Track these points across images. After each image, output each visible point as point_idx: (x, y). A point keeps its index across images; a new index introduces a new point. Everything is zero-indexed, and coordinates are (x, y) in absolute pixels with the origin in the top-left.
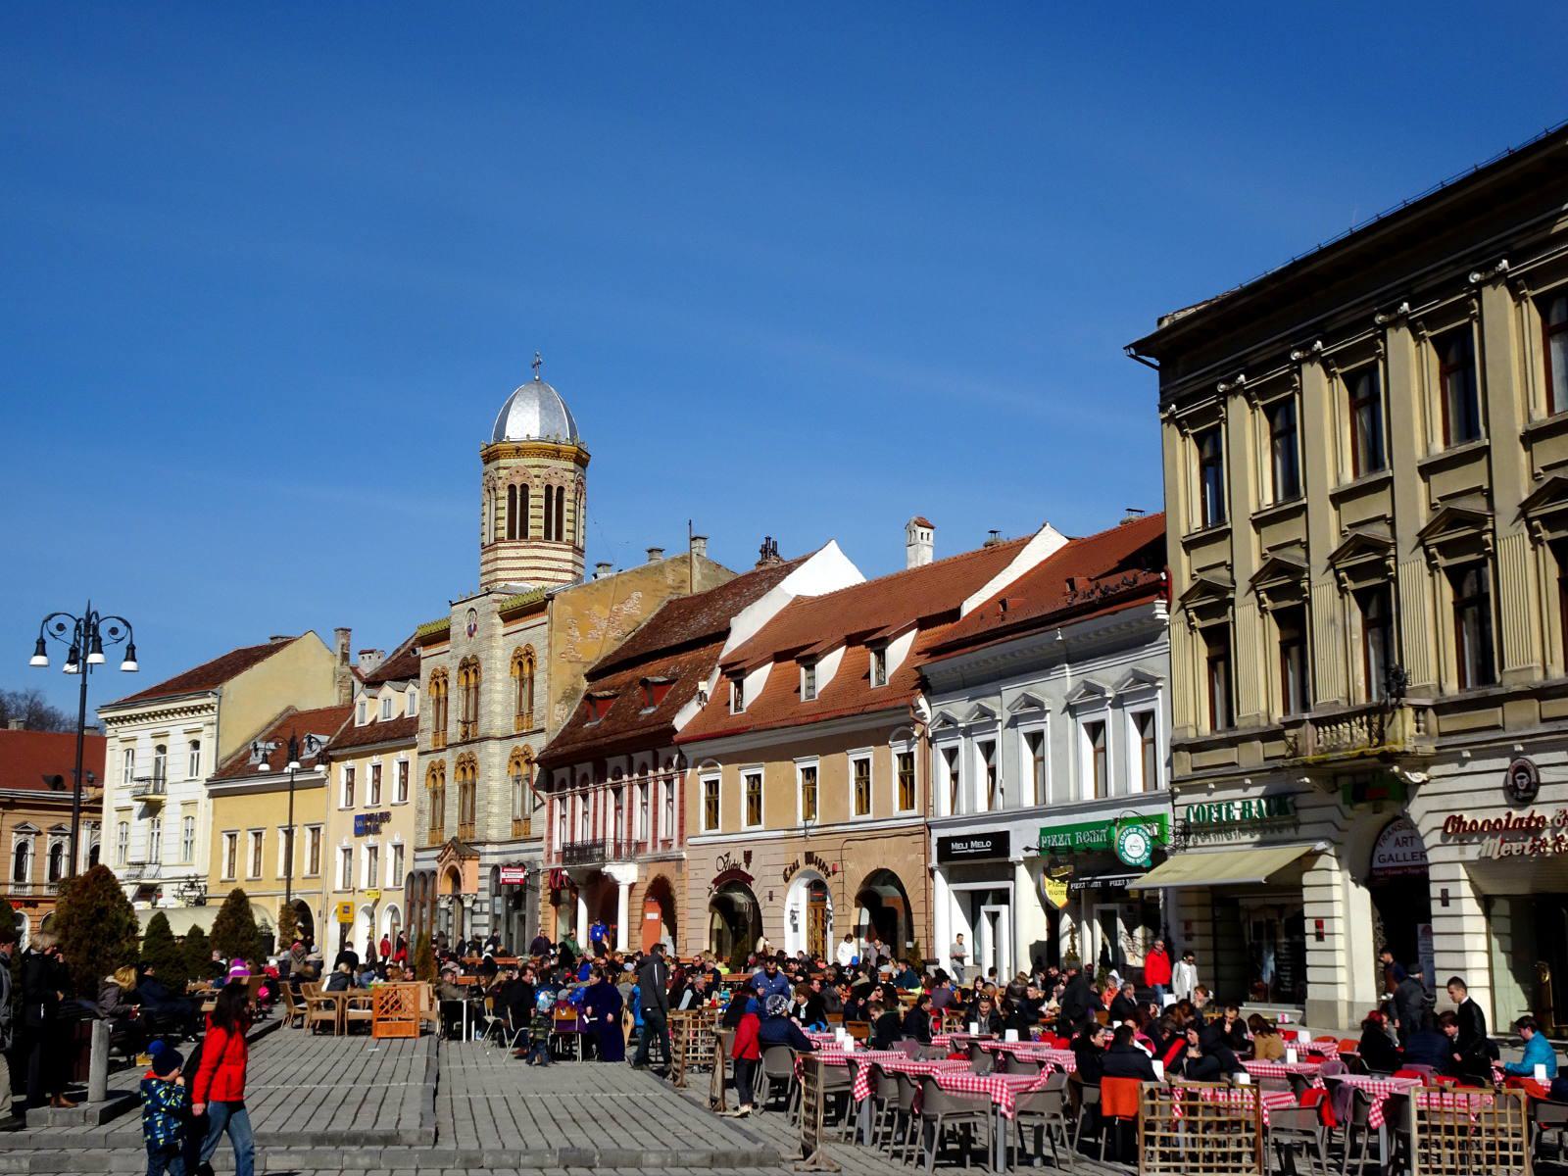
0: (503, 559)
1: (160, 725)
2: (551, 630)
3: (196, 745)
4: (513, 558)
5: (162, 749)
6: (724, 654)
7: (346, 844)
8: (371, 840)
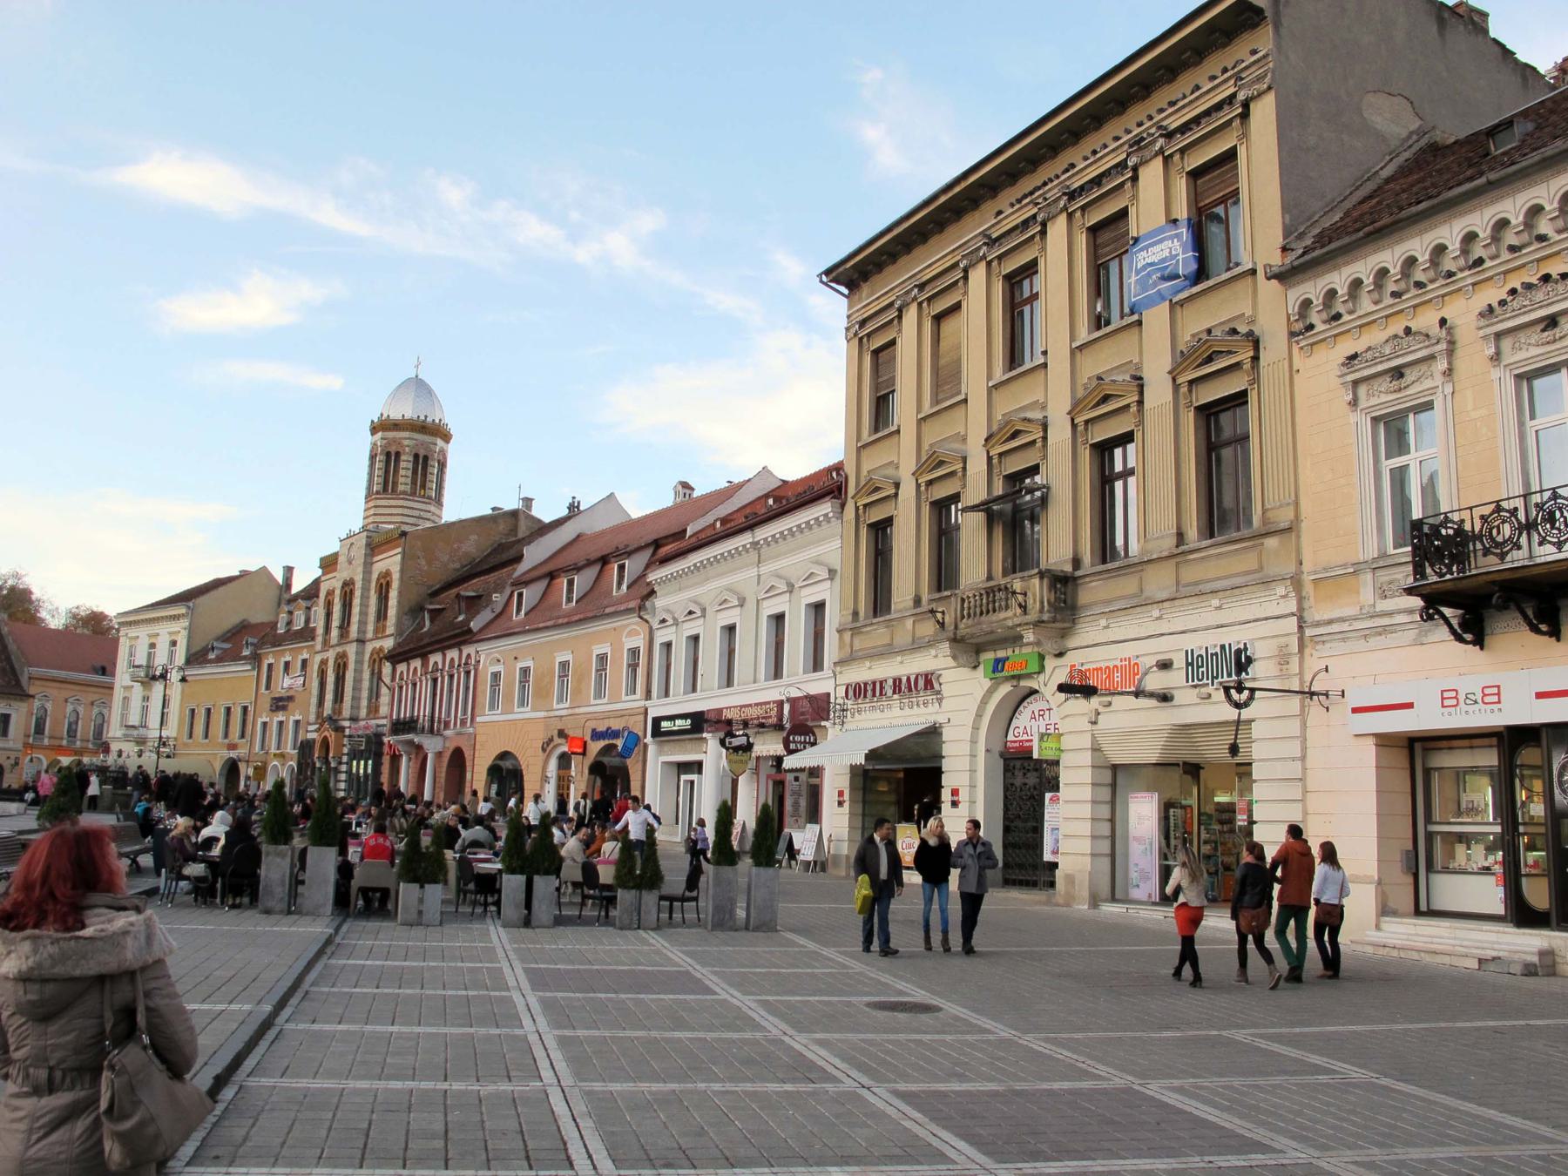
1: (155, 628)
2: (403, 558)
3: (174, 643)
5: (152, 646)
6: (516, 574)
8: (280, 717)
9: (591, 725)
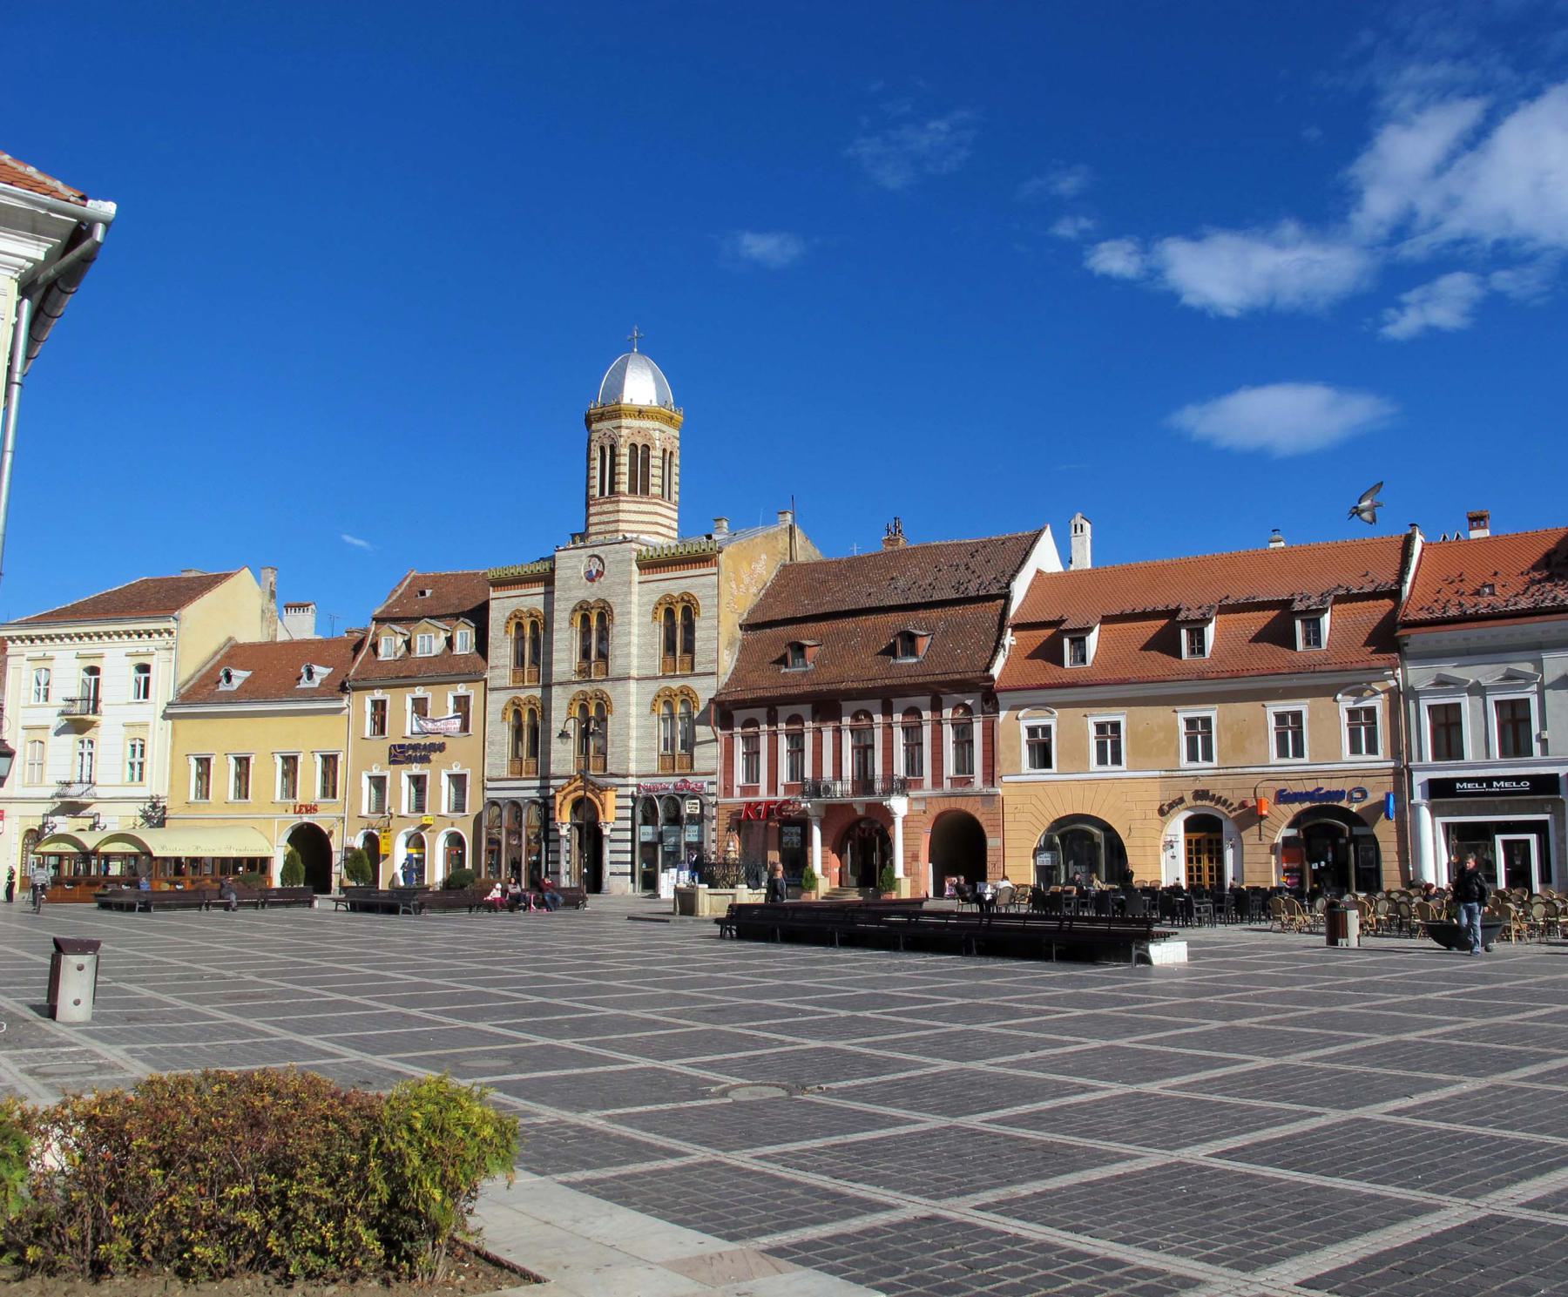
0: (623, 511)
4: (635, 512)
5: (94, 671)
7: (376, 772)
9: (1281, 785)
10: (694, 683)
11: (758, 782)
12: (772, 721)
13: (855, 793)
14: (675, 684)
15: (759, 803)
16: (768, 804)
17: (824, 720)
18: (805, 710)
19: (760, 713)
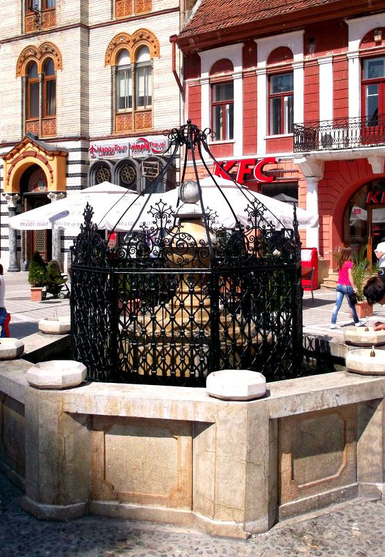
10: (149, 24)
11: (231, 137)
12: (250, 59)
13: (366, 138)
14: (130, 28)
15: (233, 164)
16: (246, 164)
17: (322, 48)
18: (294, 40)
19: (234, 52)
